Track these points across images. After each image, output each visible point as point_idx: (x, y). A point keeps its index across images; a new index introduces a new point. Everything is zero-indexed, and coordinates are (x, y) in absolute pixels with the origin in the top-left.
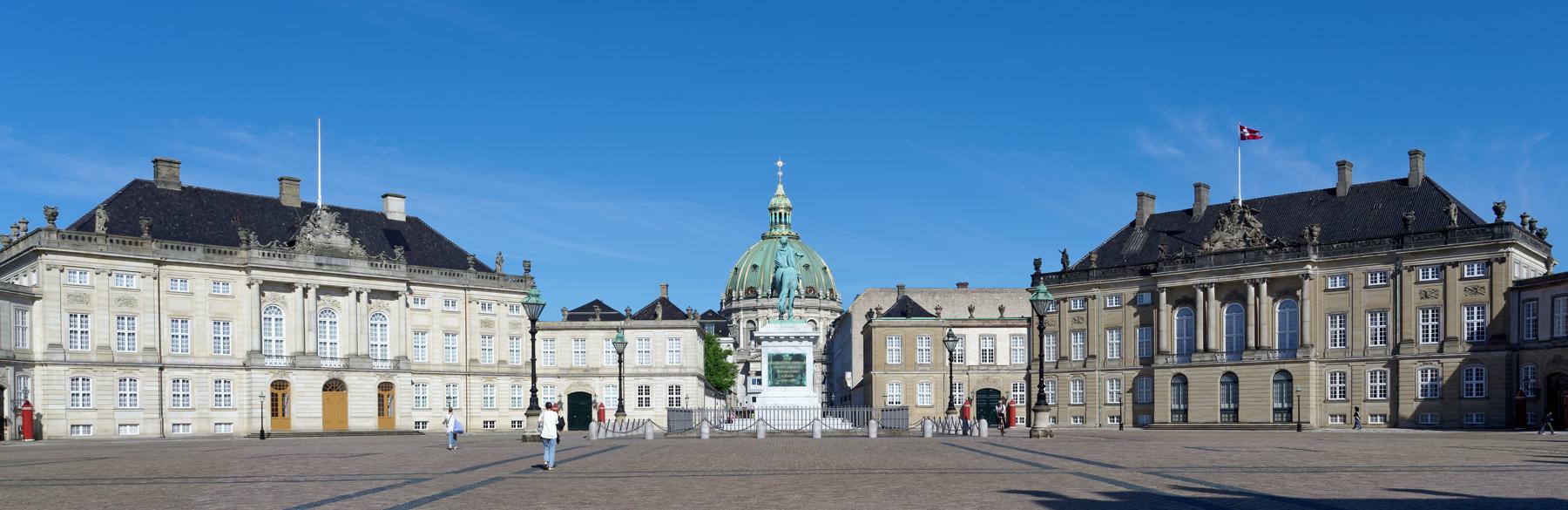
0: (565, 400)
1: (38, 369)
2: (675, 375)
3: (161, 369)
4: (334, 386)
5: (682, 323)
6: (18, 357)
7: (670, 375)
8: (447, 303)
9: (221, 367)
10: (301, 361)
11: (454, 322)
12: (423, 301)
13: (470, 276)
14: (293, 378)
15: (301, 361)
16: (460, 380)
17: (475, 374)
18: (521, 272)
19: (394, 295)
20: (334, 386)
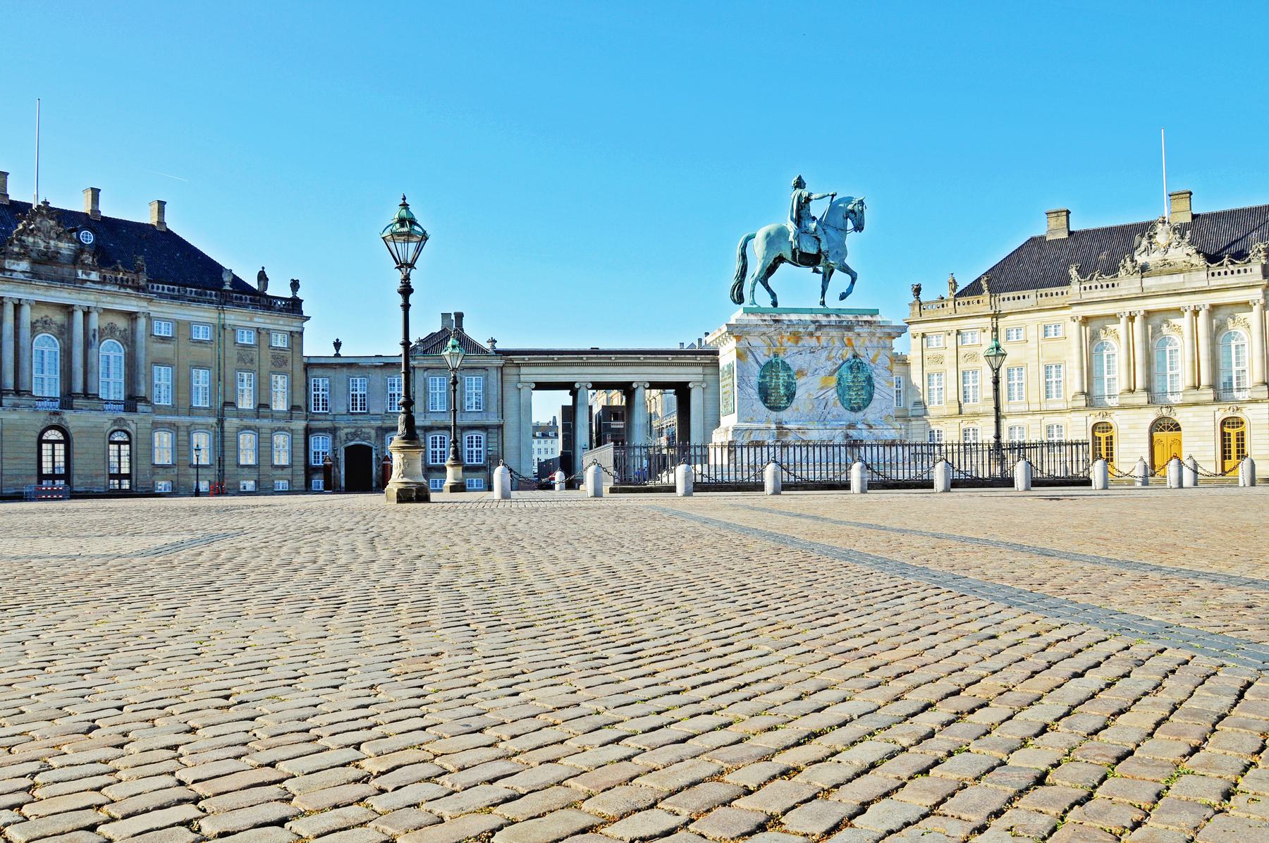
10: (1130, 399)
14: (1116, 419)
15: (1130, 399)
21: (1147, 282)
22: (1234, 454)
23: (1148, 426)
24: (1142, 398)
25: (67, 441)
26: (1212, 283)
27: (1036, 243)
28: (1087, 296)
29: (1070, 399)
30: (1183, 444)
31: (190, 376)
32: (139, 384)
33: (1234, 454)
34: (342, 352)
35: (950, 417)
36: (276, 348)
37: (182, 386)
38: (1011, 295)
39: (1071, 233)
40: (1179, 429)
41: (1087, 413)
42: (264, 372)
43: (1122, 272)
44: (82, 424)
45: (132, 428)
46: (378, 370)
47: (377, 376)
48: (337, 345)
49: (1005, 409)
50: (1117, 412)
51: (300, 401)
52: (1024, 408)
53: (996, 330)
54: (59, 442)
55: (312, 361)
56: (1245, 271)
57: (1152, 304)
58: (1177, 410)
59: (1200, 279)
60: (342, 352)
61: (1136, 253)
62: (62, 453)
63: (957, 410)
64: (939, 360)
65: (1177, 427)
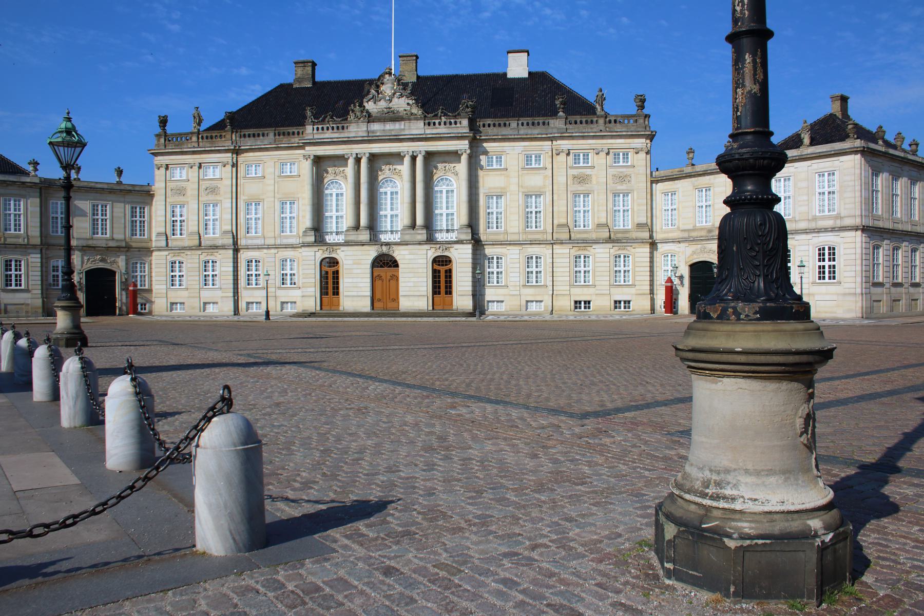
0: (685, 271)
1: (155, 254)
2: (826, 230)
3: (236, 251)
4: (385, 263)
5: (838, 146)
6: (134, 245)
7: (819, 231)
8: (528, 158)
9: (287, 247)
10: (353, 237)
11: (536, 181)
12: (499, 159)
13: (557, 123)
14: (342, 255)
15: (353, 237)
16: (544, 251)
17: (561, 243)
18: (633, 110)
19: (454, 156)
20: (385, 263)
21: (376, 127)
22: (443, 290)
23: (370, 262)
24: (365, 236)
26: (430, 131)
27: (284, 89)
28: (319, 136)
29: (301, 234)
30: (401, 280)
33: (443, 290)
35: (190, 248)
38: (251, 131)
39: (314, 83)
40: (397, 266)
41: (316, 249)
43: (351, 116)
49: (242, 242)
50: (343, 248)
52: (260, 242)
53: (235, 165)
56: (456, 123)
57: (377, 148)
58: (395, 247)
59: (417, 128)
61: (365, 100)
63: (197, 242)
64: (181, 192)
65: (395, 264)
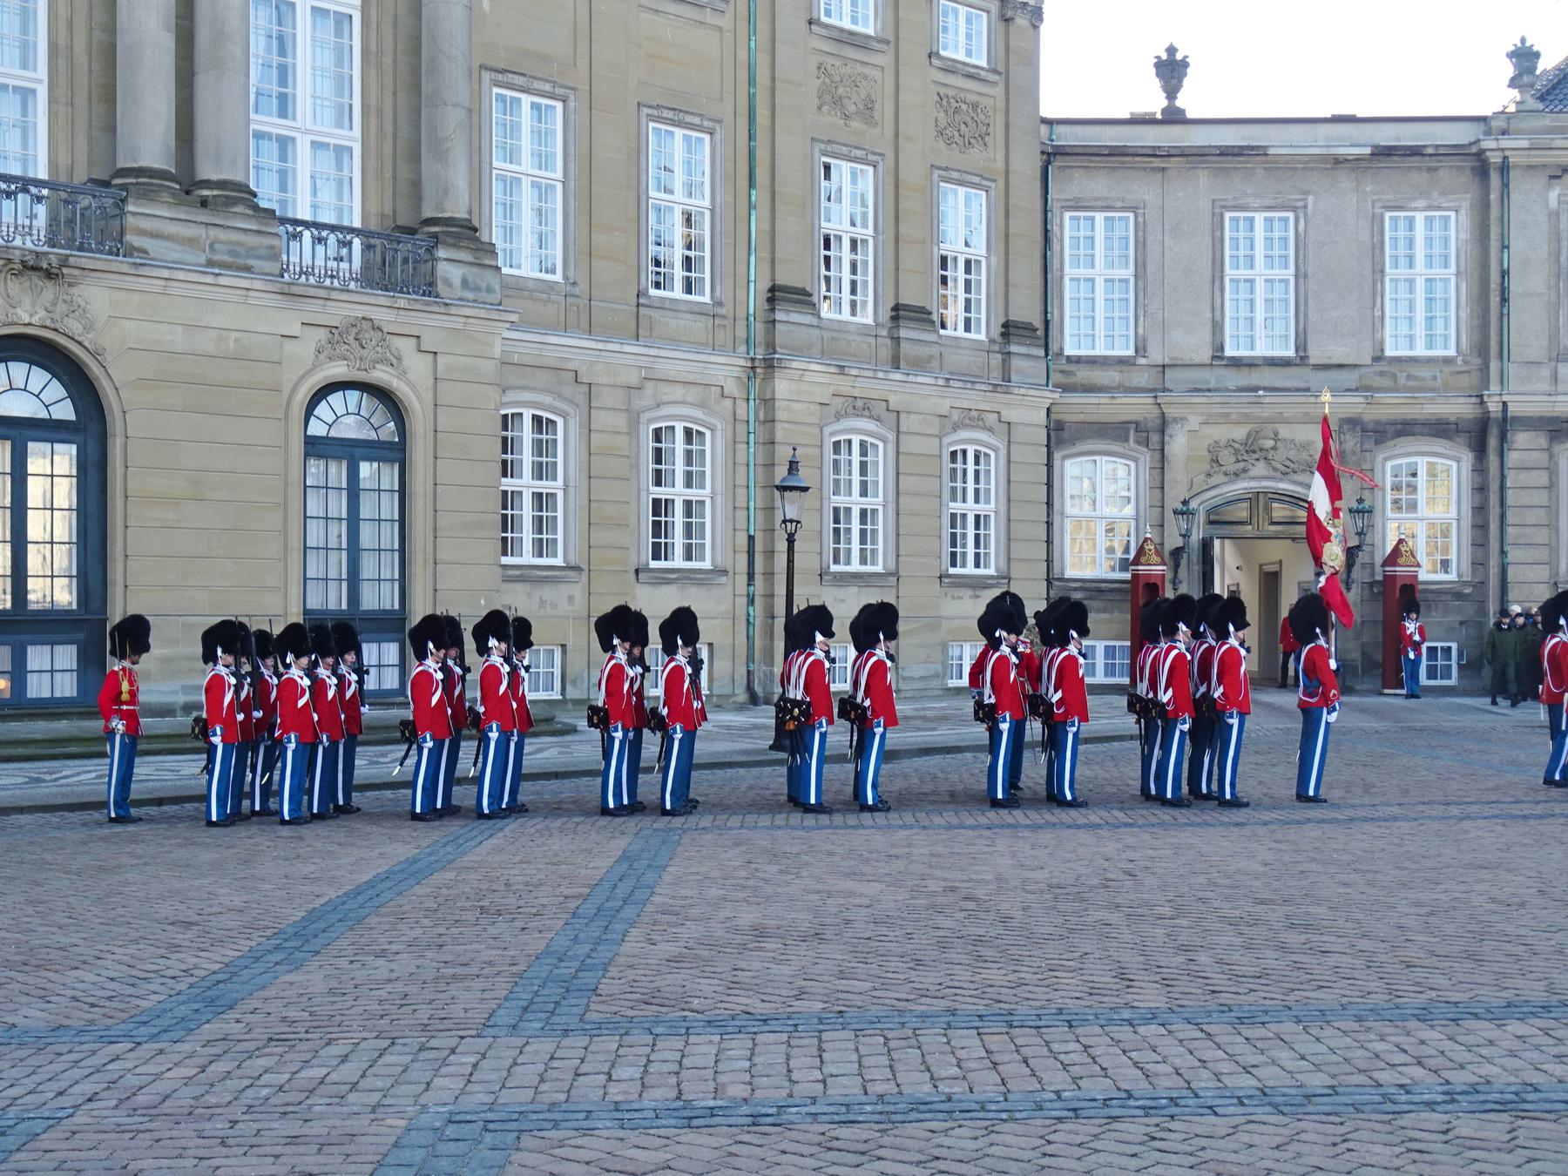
25: (90, 428)
31: (638, 152)
32: (441, 156)
34: (1192, 101)
36: (952, 68)
37: (603, 193)
42: (912, 171)
44: (175, 339)
45: (410, 379)
46: (1345, 181)
47: (1342, 203)
48: (1171, 70)
51: (1026, 311)
54: (49, 430)
55: (1066, 137)
60: (1192, 101)
62: (65, 494)
